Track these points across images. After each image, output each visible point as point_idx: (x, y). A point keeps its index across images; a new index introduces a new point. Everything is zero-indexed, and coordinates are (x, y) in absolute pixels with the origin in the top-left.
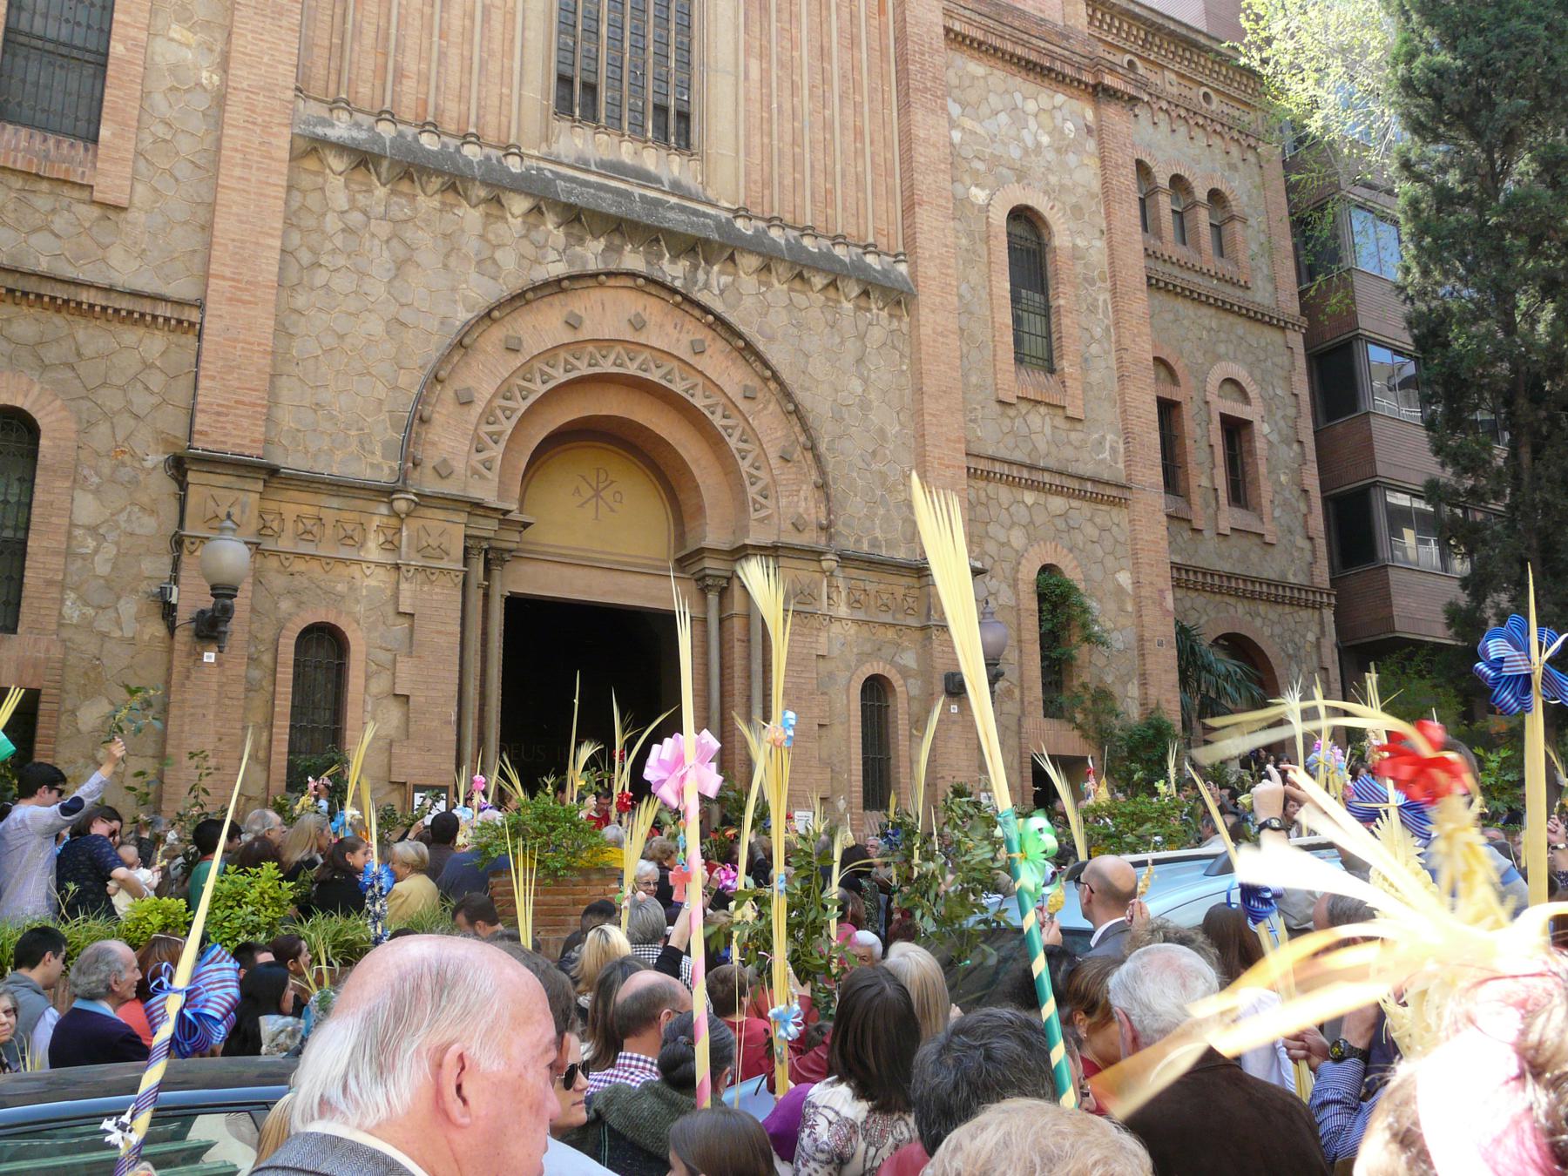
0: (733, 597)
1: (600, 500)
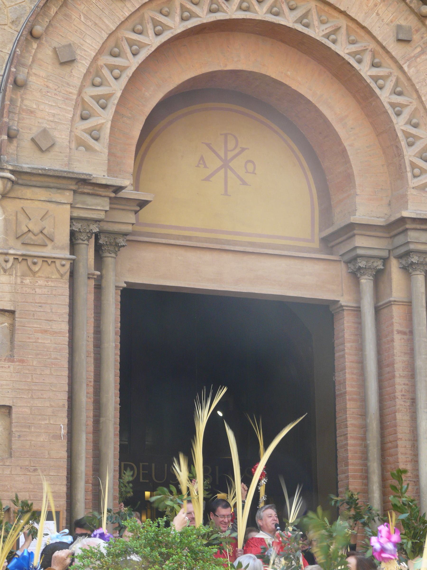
0: (390, 280)
1: (229, 172)
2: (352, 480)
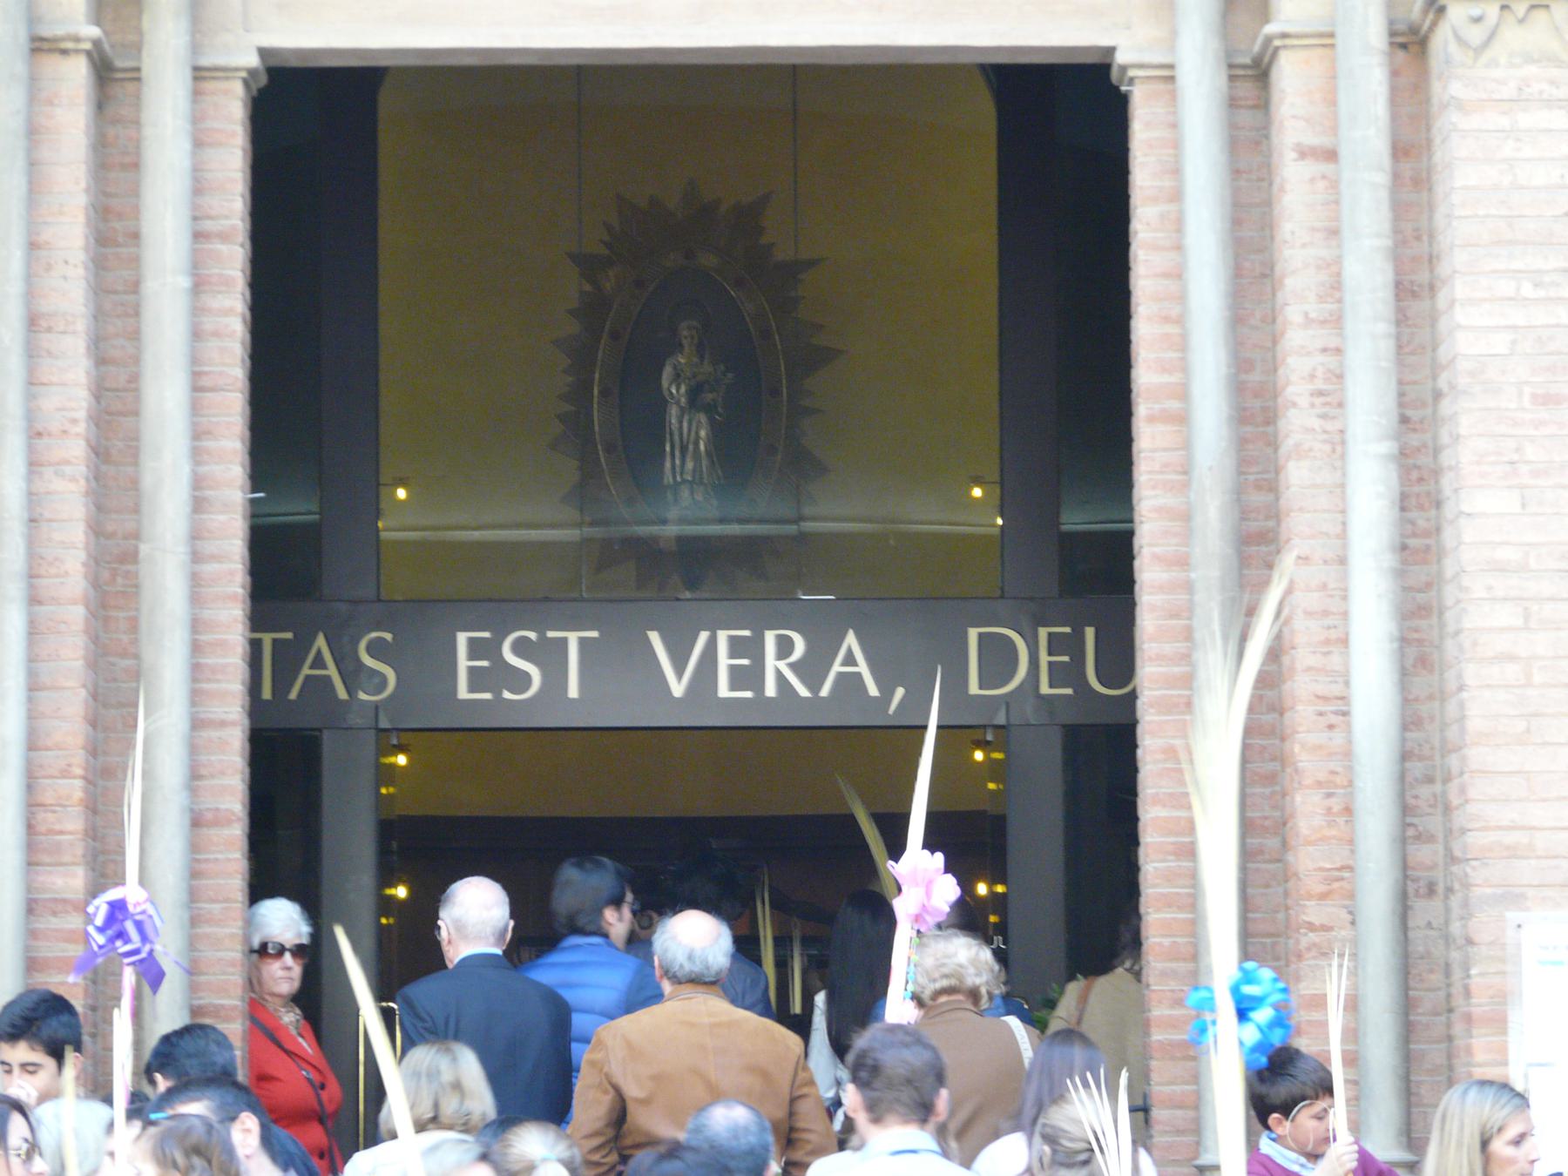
2: (1156, 718)
